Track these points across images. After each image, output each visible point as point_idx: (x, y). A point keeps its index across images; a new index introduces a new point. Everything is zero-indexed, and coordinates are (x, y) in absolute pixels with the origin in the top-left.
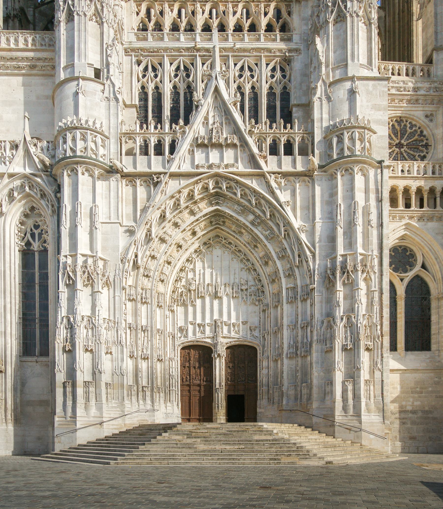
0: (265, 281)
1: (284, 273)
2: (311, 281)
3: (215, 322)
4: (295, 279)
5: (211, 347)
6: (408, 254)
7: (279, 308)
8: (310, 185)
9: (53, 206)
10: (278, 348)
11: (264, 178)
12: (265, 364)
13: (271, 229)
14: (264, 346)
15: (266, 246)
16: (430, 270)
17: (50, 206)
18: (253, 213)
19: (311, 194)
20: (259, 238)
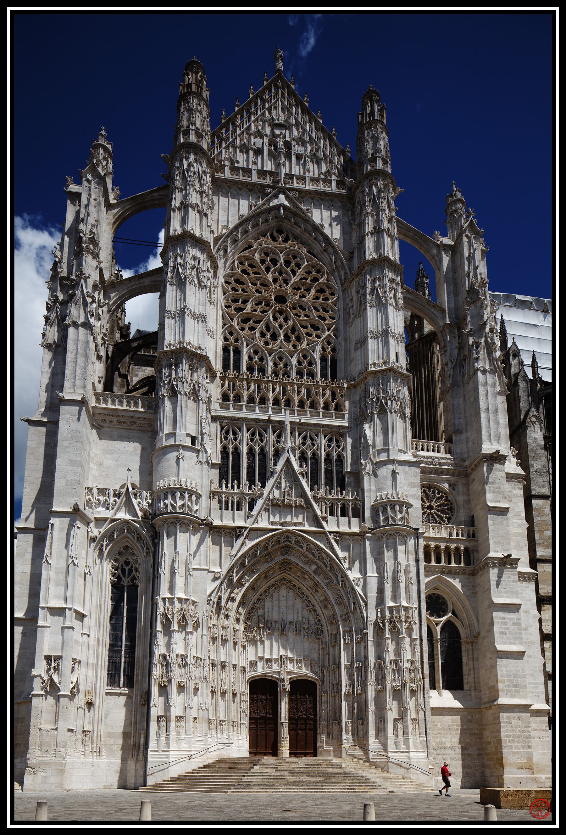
0: (324, 622)
1: (341, 617)
2: (364, 627)
3: (281, 657)
4: (350, 623)
5: (277, 681)
6: (440, 601)
7: (337, 647)
8: (362, 543)
9: (147, 549)
10: (337, 684)
11: (326, 536)
12: (324, 699)
13: (331, 579)
14: (323, 682)
15: (325, 592)
16: (459, 616)
17: (145, 549)
18: (316, 564)
19: (362, 551)
20: (320, 584)
